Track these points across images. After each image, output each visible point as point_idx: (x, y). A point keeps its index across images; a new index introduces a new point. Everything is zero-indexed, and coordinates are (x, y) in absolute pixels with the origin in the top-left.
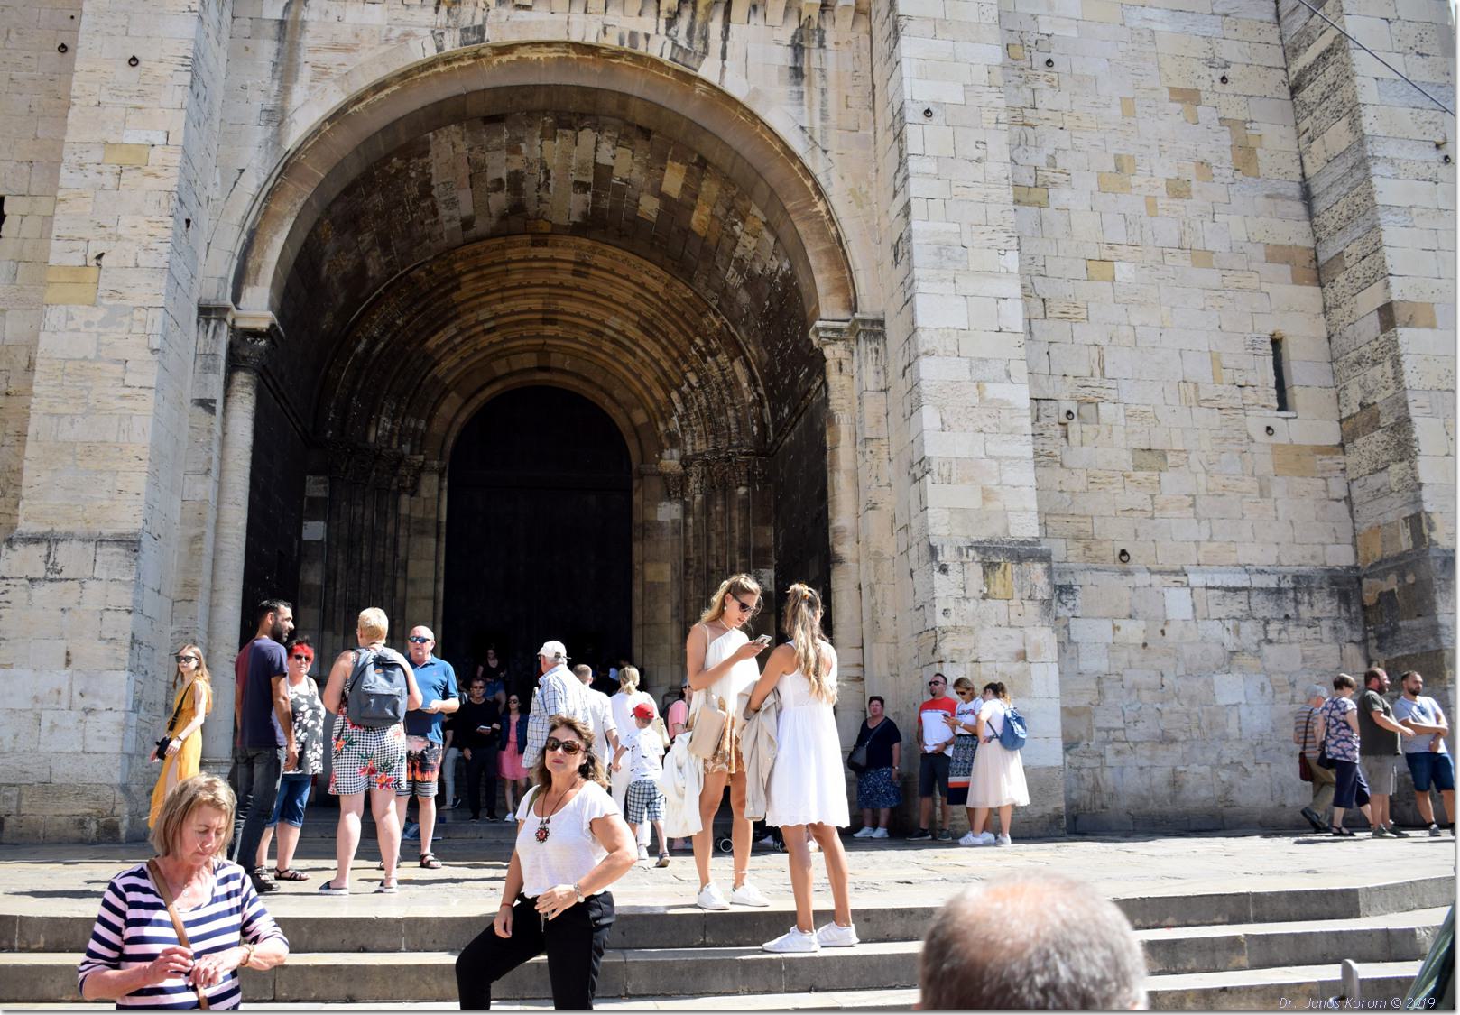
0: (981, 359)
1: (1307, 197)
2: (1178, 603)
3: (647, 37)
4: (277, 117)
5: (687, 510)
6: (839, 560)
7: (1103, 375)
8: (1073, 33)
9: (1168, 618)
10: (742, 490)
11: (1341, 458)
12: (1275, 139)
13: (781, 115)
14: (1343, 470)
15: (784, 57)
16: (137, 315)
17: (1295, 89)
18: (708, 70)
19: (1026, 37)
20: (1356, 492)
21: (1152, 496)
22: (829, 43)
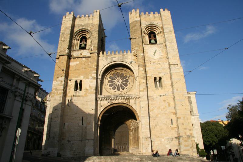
4: (100, 110)
5: (133, 133)
12: (172, 103)
13: (134, 106)
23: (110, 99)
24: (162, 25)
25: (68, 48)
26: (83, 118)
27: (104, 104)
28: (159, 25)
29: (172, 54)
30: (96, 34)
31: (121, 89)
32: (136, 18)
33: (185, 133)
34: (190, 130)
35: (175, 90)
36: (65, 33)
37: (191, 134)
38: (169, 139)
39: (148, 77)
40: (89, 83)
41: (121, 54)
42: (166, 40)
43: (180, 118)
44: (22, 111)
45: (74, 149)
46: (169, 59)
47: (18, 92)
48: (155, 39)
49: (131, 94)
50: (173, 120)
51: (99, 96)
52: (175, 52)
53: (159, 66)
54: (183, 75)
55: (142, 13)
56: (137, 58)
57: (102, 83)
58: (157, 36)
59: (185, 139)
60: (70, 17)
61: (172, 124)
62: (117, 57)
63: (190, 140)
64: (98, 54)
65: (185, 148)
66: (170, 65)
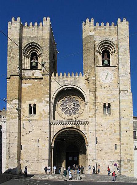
2: (107, 162)
4: (53, 133)
12: (118, 129)
15: (84, 127)
23: (63, 123)
24: (117, 42)
26: (38, 140)
27: (57, 129)
33: (126, 158)
34: (131, 155)
39: (98, 102)
40: (43, 107)
41: (74, 77)
43: (123, 144)
45: (32, 168)
51: (52, 120)
52: (127, 76)
53: (109, 92)
54: (132, 102)
55: (97, 24)
56: (88, 82)
57: (54, 110)
61: (116, 149)
62: (69, 80)
63: (129, 164)
64: (51, 75)
65: (125, 170)
66: (120, 91)
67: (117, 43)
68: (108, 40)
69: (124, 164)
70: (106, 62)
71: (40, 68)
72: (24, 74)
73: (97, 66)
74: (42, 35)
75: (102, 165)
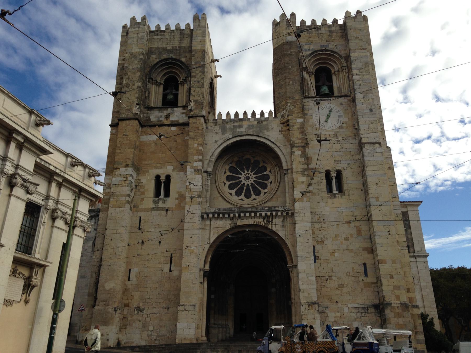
0: (308, 273)
1: (371, 239)
3: (261, 222)
6: (292, 303)
7: (333, 272)
8: (328, 214)
9: (345, 312)
10: (285, 286)
11: (377, 284)
12: (364, 228)
14: (377, 286)
15: (281, 223)
16: (194, 273)
17: (369, 219)
18: (270, 227)
19: (320, 215)
20: (379, 291)
21: (342, 292)
22: (288, 220)
23: (232, 215)
25: (137, 104)
28: (340, 50)
29: (368, 119)
30: (200, 72)
31: (252, 193)
32: (290, 35)
33: (398, 297)
34: (408, 290)
35: (372, 200)
36: (130, 67)
37: (411, 300)
38: (359, 307)
42: (356, 87)
44: (66, 247)
46: (361, 132)
47: (61, 211)
48: (329, 84)
49: (275, 207)
50: (367, 265)
58: (334, 78)
59: (397, 311)
60: (140, 29)
61: (366, 274)
62: (245, 126)
67: (346, 54)
68: (327, 48)
69: (393, 314)
70: (325, 89)
71: (184, 105)
72: (148, 116)
73: (305, 97)
74: (188, 45)
75: (335, 317)
